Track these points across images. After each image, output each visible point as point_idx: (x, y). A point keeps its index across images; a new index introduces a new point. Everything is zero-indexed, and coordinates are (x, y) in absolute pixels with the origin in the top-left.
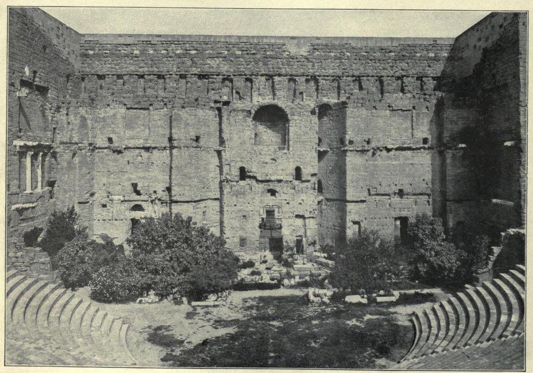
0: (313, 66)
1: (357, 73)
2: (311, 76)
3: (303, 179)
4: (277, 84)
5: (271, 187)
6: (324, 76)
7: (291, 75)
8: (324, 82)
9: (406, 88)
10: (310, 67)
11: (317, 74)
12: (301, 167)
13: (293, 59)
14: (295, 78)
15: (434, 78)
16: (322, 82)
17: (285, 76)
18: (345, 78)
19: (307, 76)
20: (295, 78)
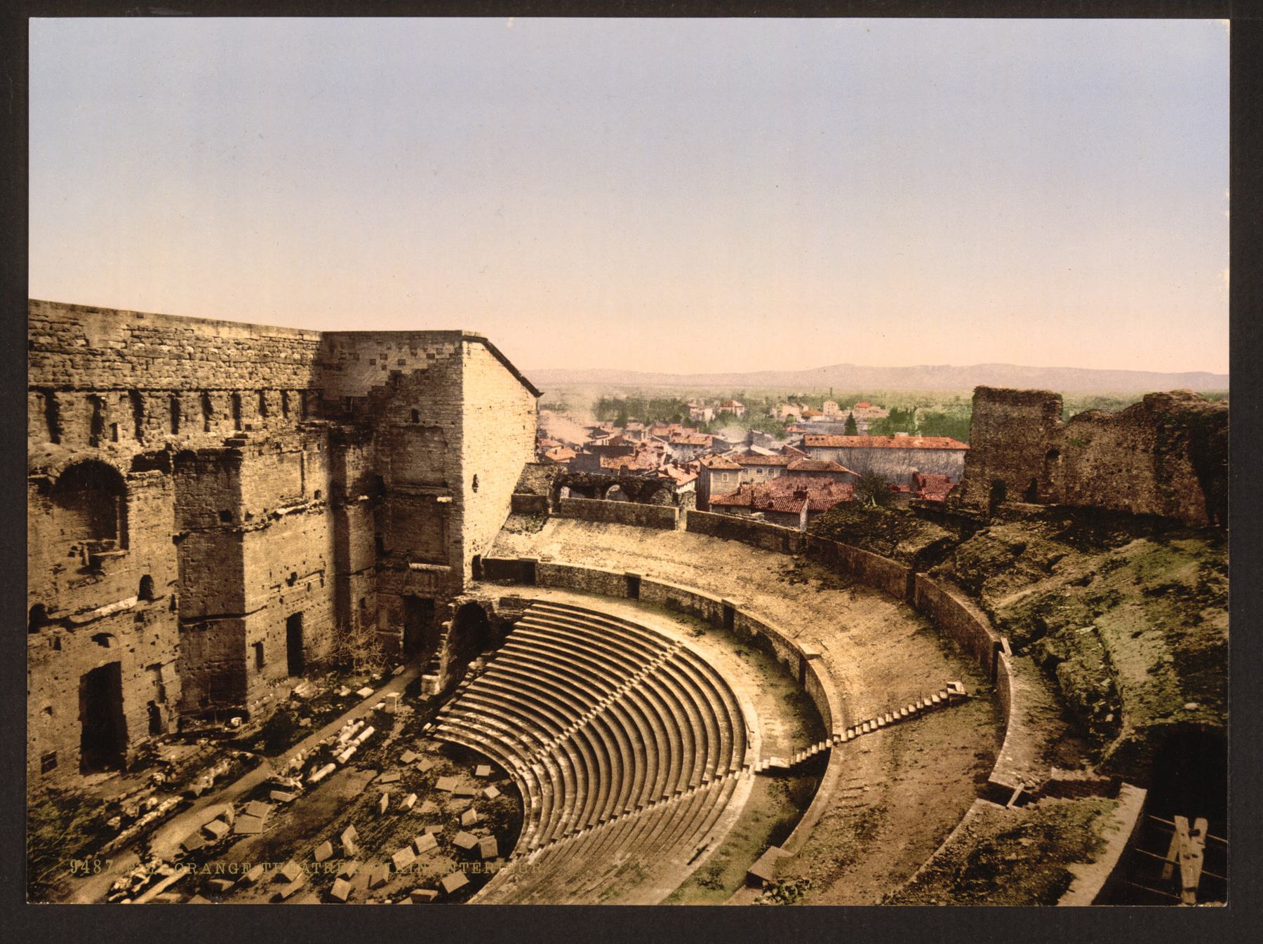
0: (133, 369)
1: (204, 385)
2: (130, 391)
3: (156, 596)
4: (66, 410)
5: (101, 630)
6: (154, 390)
7: (93, 389)
8: (153, 400)
9: (270, 409)
10: (127, 372)
11: (140, 386)
12: (152, 574)
13: (94, 355)
14: (98, 394)
15: (299, 391)
16: (149, 403)
17: (78, 391)
18: (185, 393)
19: (123, 390)
20: (98, 394)
